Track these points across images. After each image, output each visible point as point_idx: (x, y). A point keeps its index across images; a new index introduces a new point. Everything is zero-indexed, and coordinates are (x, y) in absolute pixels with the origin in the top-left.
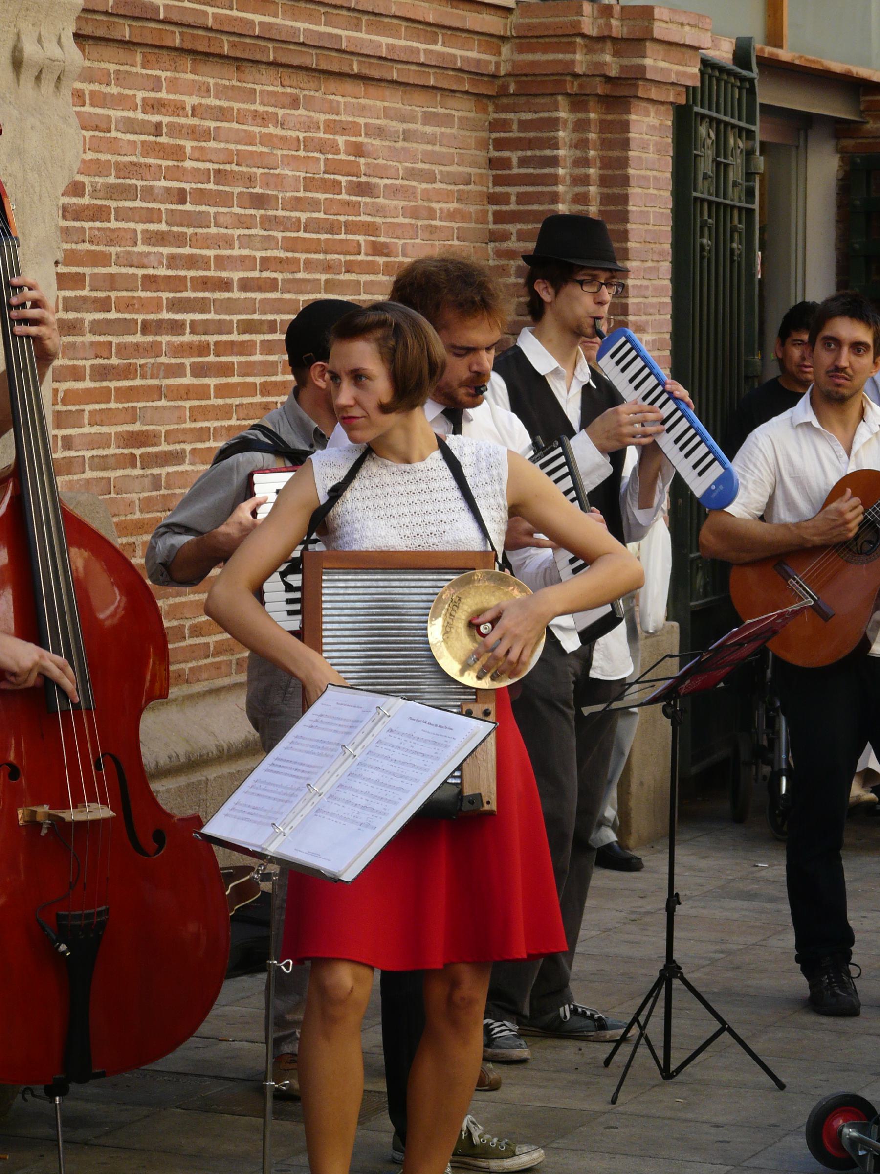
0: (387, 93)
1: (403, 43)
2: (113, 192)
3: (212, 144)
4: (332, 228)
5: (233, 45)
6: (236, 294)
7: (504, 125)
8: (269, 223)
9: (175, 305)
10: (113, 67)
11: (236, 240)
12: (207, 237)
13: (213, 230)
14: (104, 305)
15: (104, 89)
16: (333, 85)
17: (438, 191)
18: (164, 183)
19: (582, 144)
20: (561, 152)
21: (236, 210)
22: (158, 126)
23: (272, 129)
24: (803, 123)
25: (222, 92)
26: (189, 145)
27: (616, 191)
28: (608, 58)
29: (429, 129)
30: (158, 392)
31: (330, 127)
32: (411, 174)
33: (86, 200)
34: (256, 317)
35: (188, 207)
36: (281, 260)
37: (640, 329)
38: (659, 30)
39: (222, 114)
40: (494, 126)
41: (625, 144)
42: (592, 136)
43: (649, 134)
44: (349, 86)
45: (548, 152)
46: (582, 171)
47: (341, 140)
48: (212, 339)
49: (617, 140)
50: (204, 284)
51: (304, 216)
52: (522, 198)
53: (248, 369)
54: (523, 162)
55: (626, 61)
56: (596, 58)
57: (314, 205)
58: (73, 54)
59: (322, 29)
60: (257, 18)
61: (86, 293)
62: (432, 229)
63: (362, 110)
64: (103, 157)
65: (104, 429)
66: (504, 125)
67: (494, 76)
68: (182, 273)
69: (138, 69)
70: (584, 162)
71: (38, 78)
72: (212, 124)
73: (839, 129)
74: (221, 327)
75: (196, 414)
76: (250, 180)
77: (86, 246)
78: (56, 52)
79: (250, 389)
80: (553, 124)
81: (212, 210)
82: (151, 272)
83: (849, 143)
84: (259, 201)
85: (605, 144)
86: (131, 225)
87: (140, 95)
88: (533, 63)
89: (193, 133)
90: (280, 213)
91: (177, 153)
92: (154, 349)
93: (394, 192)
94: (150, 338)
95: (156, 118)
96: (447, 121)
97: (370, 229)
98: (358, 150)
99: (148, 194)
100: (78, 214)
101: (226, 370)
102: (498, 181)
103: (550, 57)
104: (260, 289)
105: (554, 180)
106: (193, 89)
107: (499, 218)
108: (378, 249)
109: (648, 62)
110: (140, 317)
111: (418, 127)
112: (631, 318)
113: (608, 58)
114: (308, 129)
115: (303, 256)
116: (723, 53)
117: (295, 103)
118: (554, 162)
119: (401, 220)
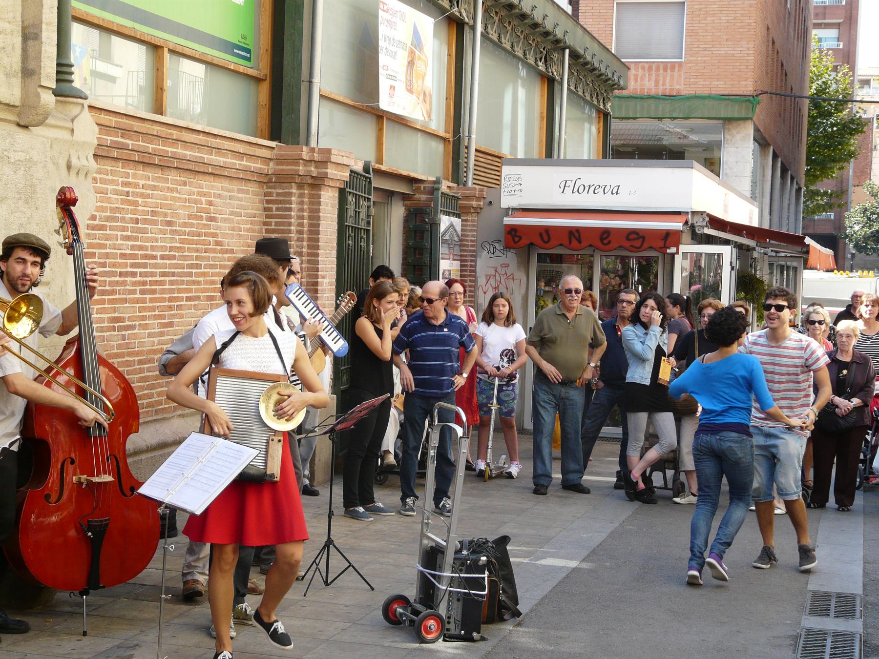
0: (223, 180)
1: (229, 160)
2: (108, 219)
3: (150, 200)
4: (199, 235)
5: (160, 160)
6: (159, 261)
7: (270, 194)
8: (173, 232)
9: (133, 265)
10: (109, 168)
11: (159, 239)
12: (147, 238)
13: (150, 235)
14: (103, 265)
16: (201, 177)
17: (242, 220)
18: (130, 216)
19: (301, 203)
20: (293, 206)
21: (160, 227)
22: (128, 192)
23: (175, 194)
24: (391, 194)
25: (155, 179)
26: (140, 200)
27: (315, 222)
28: (313, 169)
29: (240, 195)
30: (125, 301)
31: (199, 194)
32: (232, 213)
33: (97, 222)
34: (167, 270)
35: (139, 225)
36: (178, 248)
37: (323, 277)
38: (334, 158)
39: (155, 188)
40: (266, 194)
41: (319, 203)
42: (306, 200)
43: (329, 199)
44: (207, 177)
45: (288, 206)
46: (301, 214)
47: (203, 199)
48: (148, 279)
49: (315, 201)
50: (146, 257)
51: (187, 230)
52: (277, 224)
53: (163, 291)
54: (278, 209)
55: (320, 170)
56: (308, 168)
57: (192, 225)
60: (170, 149)
61: (96, 260)
62: (240, 236)
64: (104, 205)
65: (102, 316)
66: (270, 194)
68: (137, 252)
69: (120, 169)
70: (302, 210)
71: (78, 173)
72: (151, 192)
73: (404, 197)
74: (152, 274)
75: (141, 309)
76: (166, 215)
77: (97, 241)
78: (86, 163)
79: (163, 300)
80: (290, 194)
81: (150, 227)
82: (123, 252)
83: (407, 202)
84: (169, 223)
85: (311, 203)
86: (116, 232)
87: (121, 180)
88: (283, 170)
89: (142, 195)
90: (178, 228)
91: (136, 203)
92: (124, 283)
93: (225, 220)
94: (122, 279)
95: (127, 189)
96: (247, 192)
97: (214, 235)
98: (210, 203)
99: (123, 220)
100: (93, 228)
101: (154, 292)
102: (267, 217)
103: (289, 167)
104: (169, 259)
105: (290, 217)
106: (142, 177)
108: (218, 243)
109: (329, 171)
110: (118, 270)
111: (235, 194)
112: (320, 273)
113: (313, 169)
114: (190, 194)
115: (187, 246)
116: (359, 167)
117: (185, 184)
118: (290, 209)
119: (227, 232)
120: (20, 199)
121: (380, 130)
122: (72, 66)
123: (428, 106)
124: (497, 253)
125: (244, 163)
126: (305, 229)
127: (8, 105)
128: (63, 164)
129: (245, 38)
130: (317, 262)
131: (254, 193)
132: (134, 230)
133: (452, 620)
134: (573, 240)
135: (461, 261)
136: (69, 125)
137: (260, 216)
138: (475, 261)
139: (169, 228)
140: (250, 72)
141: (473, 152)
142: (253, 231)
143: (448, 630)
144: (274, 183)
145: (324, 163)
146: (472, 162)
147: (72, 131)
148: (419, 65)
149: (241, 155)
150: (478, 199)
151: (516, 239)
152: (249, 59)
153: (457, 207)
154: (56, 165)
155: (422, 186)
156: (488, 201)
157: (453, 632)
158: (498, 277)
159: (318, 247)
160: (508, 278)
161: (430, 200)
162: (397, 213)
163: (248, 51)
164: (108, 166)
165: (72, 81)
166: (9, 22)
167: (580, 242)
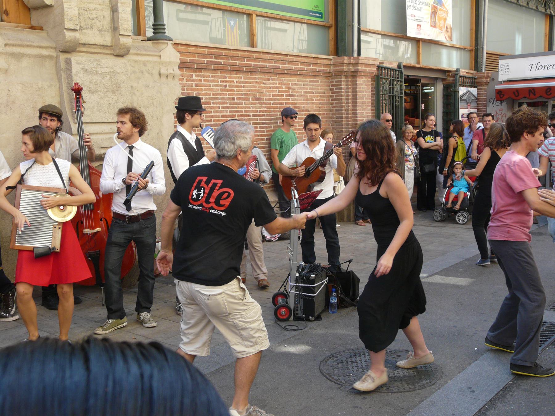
1: (300, 67)
4: (281, 104)
6: (251, 117)
10: (211, 74)
13: (244, 105)
15: (208, 79)
16: (280, 76)
19: (347, 85)
23: (262, 85)
24: (436, 79)
26: (235, 89)
29: (311, 83)
39: (246, 82)
41: (356, 84)
44: (286, 76)
47: (284, 86)
49: (354, 84)
52: (336, 96)
54: (336, 89)
58: (178, 72)
59: (274, 65)
60: (253, 63)
62: (313, 103)
63: (290, 80)
67: (329, 72)
72: (243, 85)
73: (443, 80)
76: (256, 95)
78: (172, 72)
80: (341, 81)
83: (444, 82)
89: (236, 86)
91: (233, 91)
93: (301, 96)
96: (318, 82)
98: (289, 88)
102: (332, 93)
105: (342, 92)
106: (235, 78)
107: (332, 100)
108: (295, 107)
109: (359, 68)
111: (308, 83)
117: (269, 79)
118: (341, 89)
120: (108, 91)
121: (418, 47)
122: (165, 25)
123: (449, 33)
124: (497, 104)
125: (287, 65)
126: (350, 97)
127: (103, 46)
128: (156, 72)
129: (318, 7)
130: (356, 113)
131: (321, 82)
132: (230, 103)
133: (299, 309)
134: (531, 94)
135: (478, 109)
136: (158, 54)
137: (328, 93)
138: (486, 109)
139: (258, 102)
140: (323, 24)
141: (485, 54)
142: (322, 100)
143: (297, 314)
144: (333, 76)
145: (356, 64)
146: (484, 59)
147: (160, 56)
148: (440, 14)
149: (309, 64)
150: (487, 78)
151: (502, 96)
152: (321, 17)
153: (472, 82)
154: (151, 74)
155: (451, 73)
156: (492, 78)
157: (300, 315)
158: (497, 116)
159: (356, 106)
160: (502, 116)
161: (454, 80)
162: (440, 87)
163: (321, 13)
164: (186, 73)
165: (165, 33)
166: (100, 5)
167: (535, 95)
